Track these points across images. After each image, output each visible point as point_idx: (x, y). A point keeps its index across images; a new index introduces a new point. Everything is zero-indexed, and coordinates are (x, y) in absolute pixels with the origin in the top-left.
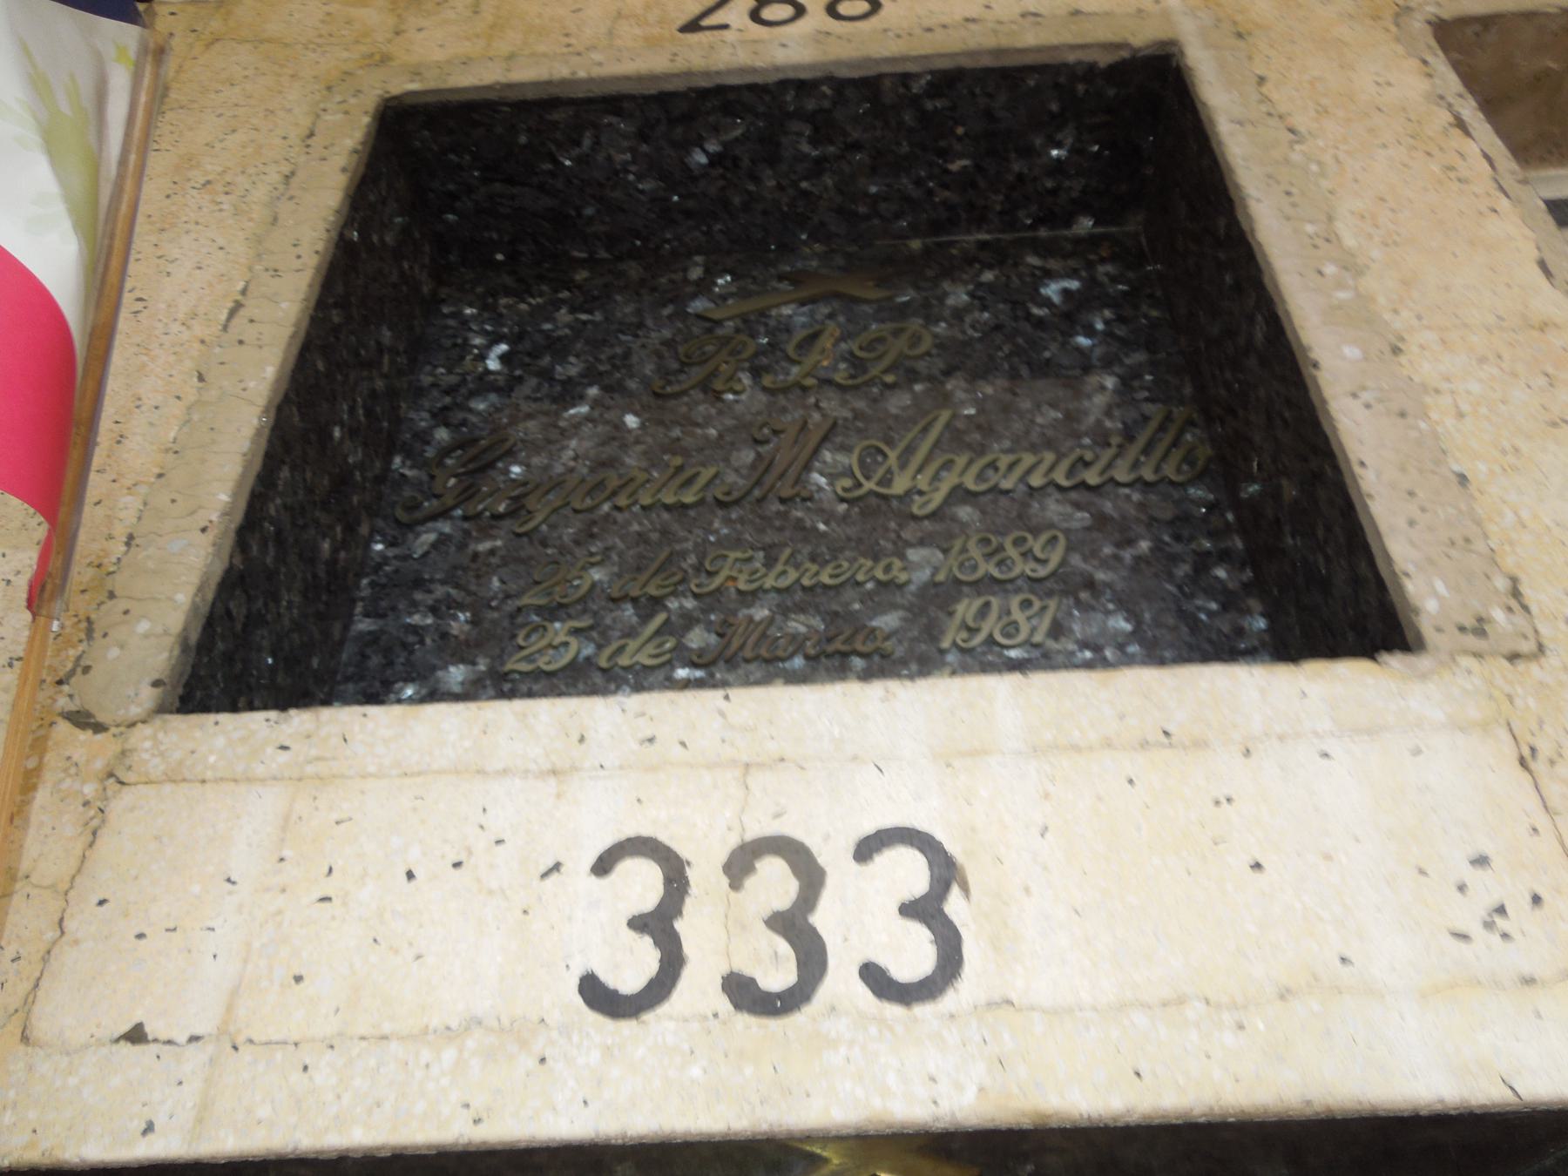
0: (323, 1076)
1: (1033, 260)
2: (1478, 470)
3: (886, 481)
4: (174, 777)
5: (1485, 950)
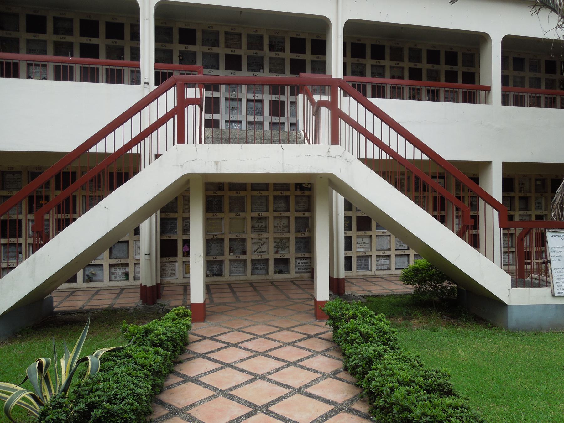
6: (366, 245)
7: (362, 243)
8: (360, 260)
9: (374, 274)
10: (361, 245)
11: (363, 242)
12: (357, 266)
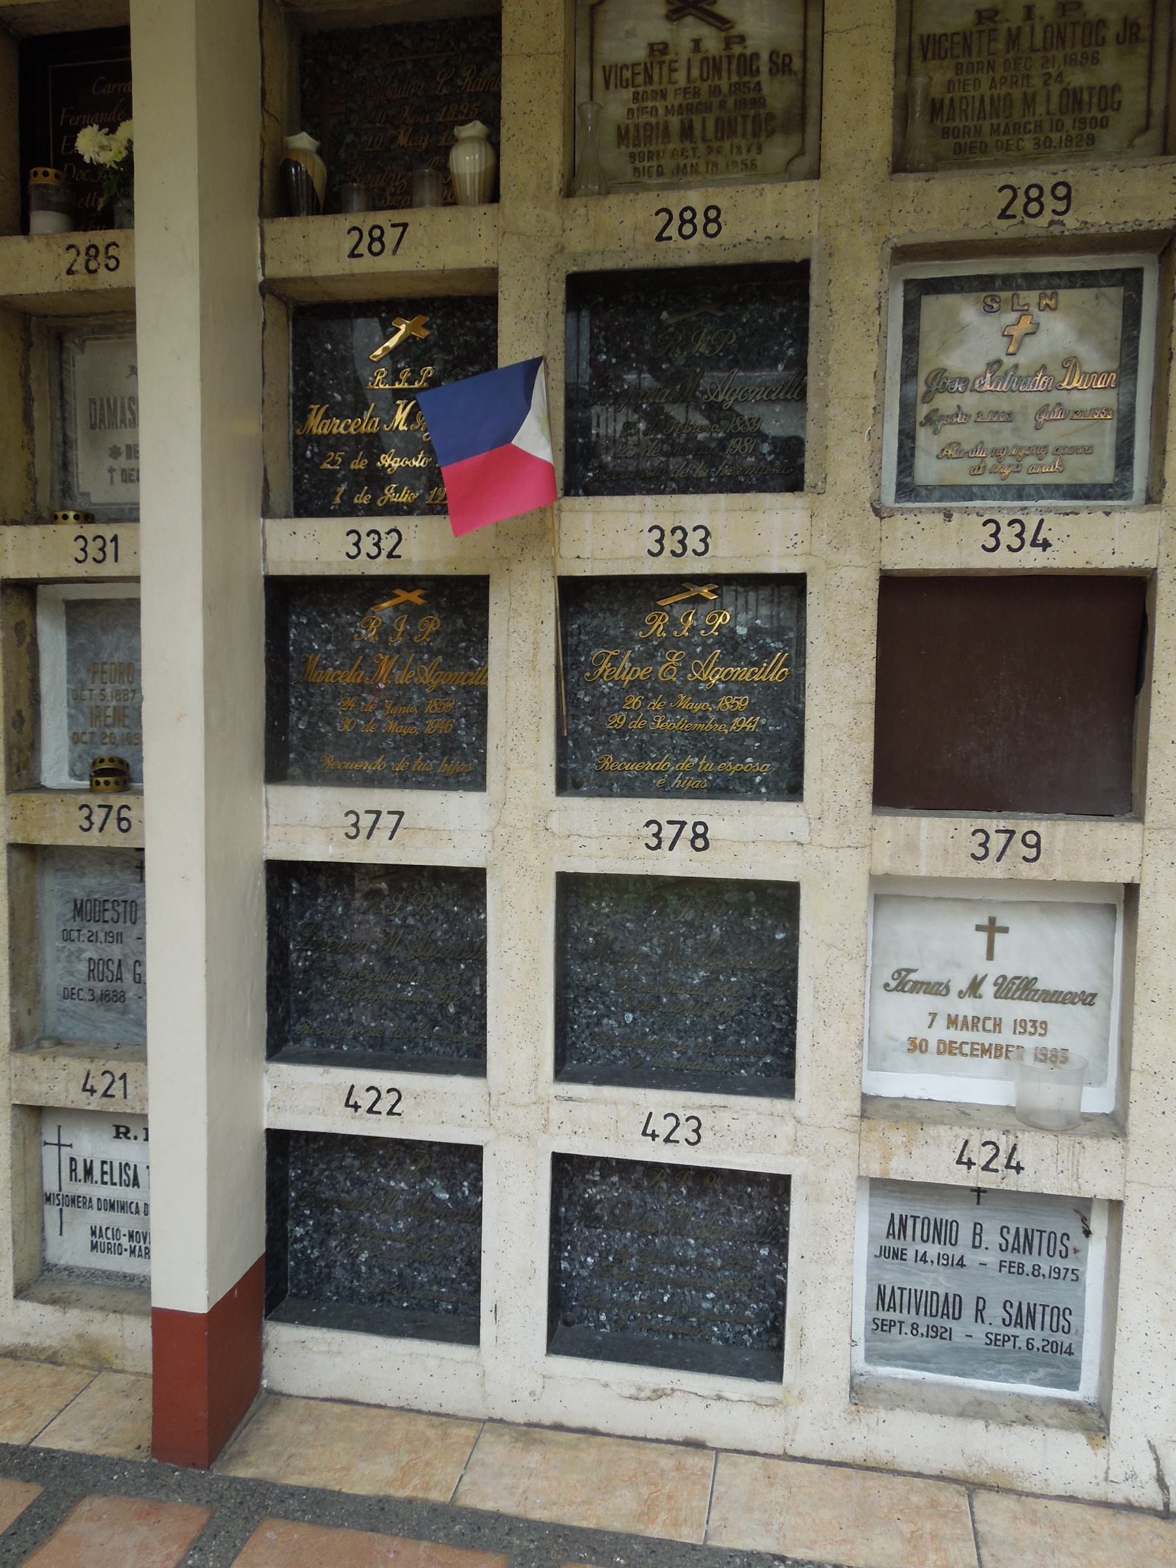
0: (610, 564)
1: (773, 298)
2: (831, 444)
3: (716, 397)
4: (571, 510)
5: (792, 551)
6: (1040, 1027)
7: (974, 987)
8: (941, 1232)
9: (1150, 1495)
10: (967, 1008)
11: (992, 971)
12: (883, 1298)
